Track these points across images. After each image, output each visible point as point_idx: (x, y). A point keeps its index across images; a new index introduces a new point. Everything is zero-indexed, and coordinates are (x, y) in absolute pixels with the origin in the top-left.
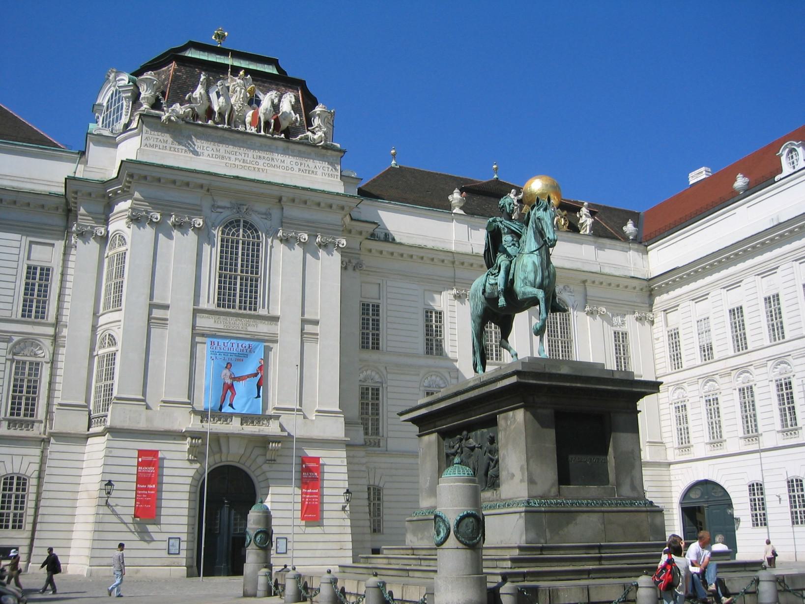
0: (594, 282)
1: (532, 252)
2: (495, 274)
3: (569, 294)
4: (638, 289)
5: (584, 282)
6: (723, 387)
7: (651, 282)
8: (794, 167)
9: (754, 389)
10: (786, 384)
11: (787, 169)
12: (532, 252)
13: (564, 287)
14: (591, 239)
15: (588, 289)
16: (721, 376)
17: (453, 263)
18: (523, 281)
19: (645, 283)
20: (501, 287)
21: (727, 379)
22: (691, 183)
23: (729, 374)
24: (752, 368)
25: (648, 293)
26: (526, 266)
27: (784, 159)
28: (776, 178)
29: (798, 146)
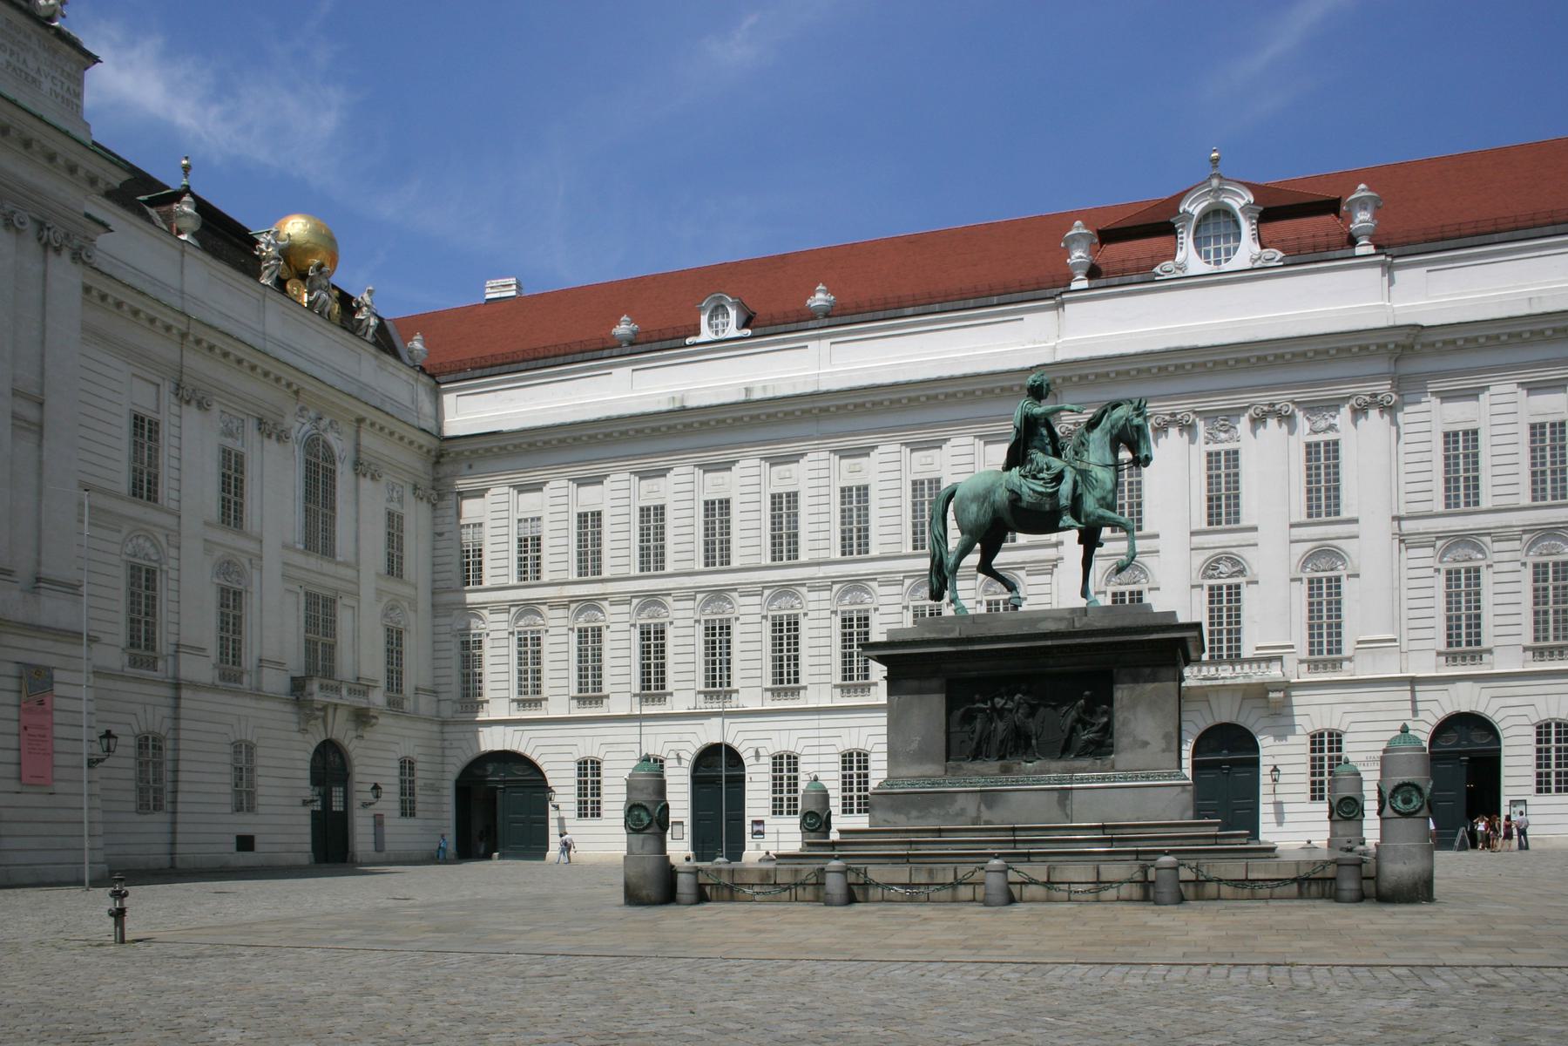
0: (372, 424)
1: (1106, 466)
2: (1043, 479)
3: (336, 435)
4: (425, 449)
5: (360, 420)
6: (552, 623)
7: (446, 445)
8: (717, 333)
9: (606, 634)
10: (656, 632)
11: (706, 334)
12: (1106, 466)
13: (331, 423)
14: (372, 349)
15: (362, 434)
16: (551, 607)
17: (184, 335)
18: (1098, 500)
19: (436, 443)
20: (1064, 501)
21: (561, 613)
22: (488, 297)
23: (566, 606)
24: (605, 604)
25: (434, 459)
26: (1105, 483)
27: (704, 319)
28: (688, 341)
29: (732, 305)
